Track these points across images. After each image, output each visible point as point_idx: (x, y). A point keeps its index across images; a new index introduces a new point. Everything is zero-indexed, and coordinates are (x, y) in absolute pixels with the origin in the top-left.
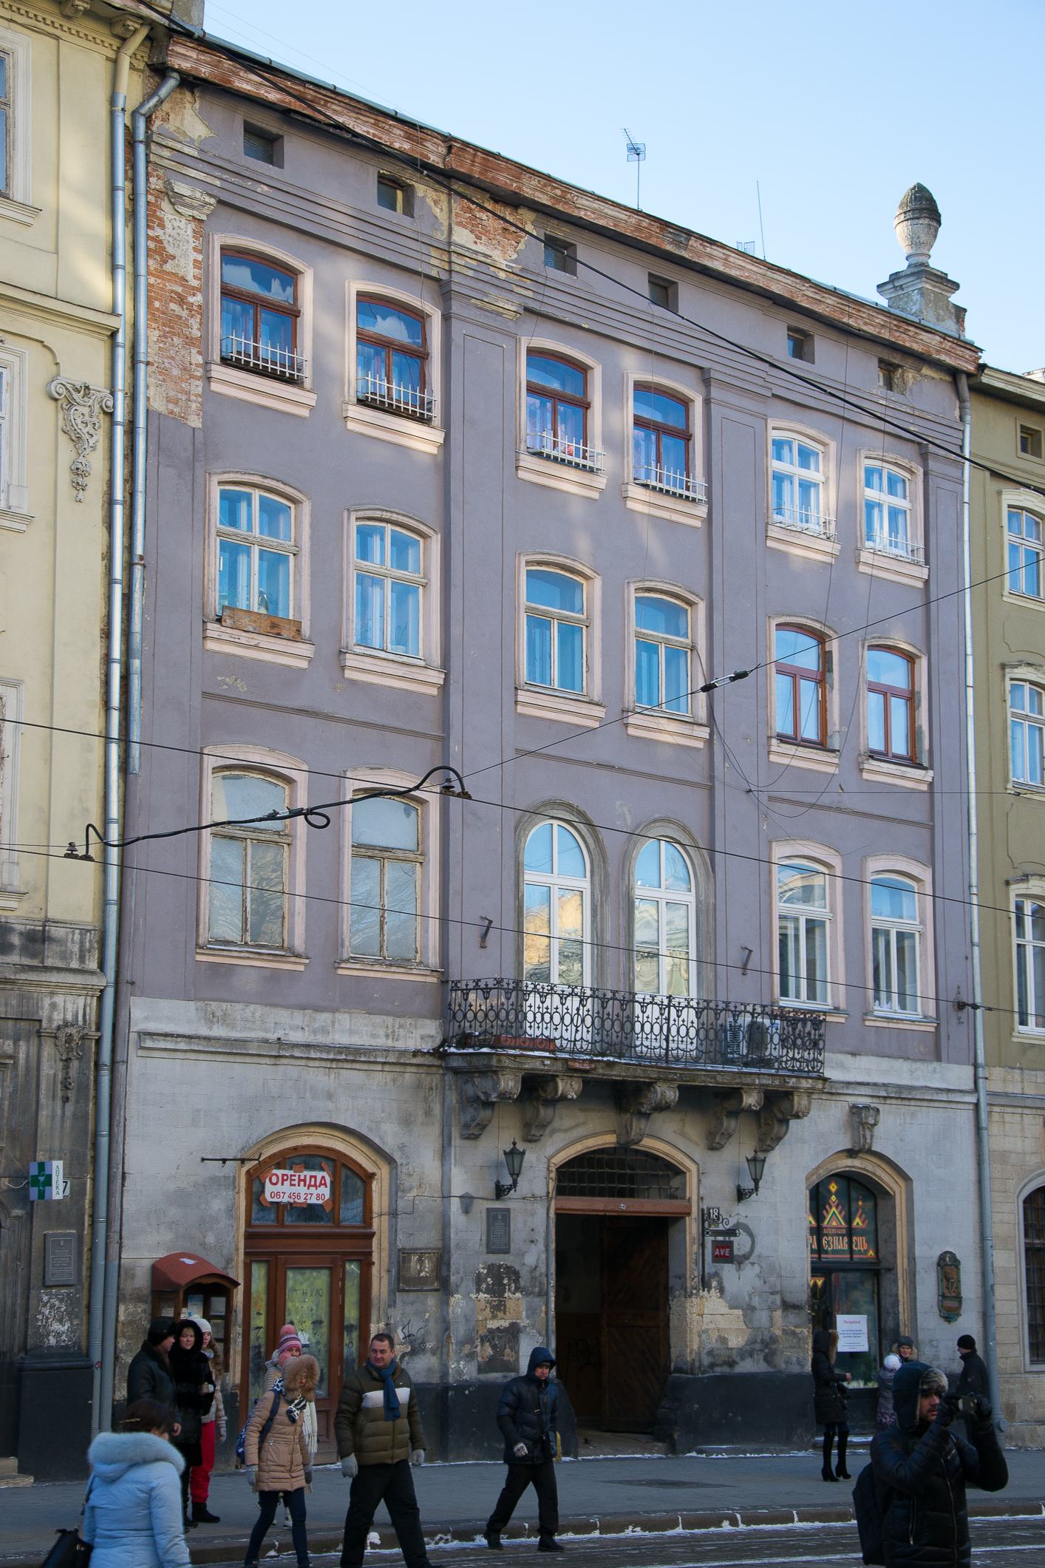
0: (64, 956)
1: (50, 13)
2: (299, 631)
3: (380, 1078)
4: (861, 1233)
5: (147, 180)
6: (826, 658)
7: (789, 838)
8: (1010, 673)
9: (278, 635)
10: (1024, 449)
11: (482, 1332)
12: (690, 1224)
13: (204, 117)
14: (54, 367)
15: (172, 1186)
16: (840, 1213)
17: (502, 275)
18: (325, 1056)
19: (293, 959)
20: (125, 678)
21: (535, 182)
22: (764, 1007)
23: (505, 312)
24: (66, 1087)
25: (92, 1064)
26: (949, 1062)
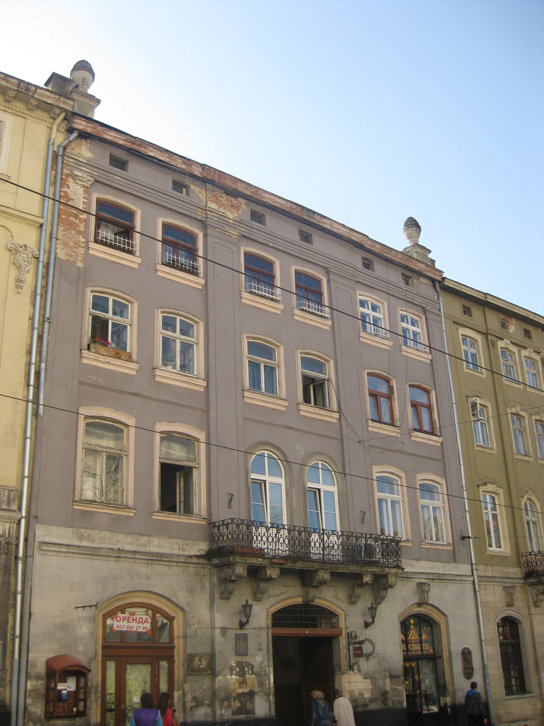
1: (21, 108)
2: (130, 357)
3: (175, 570)
4: (426, 641)
5: (62, 170)
6: (391, 388)
7: (380, 464)
9: (119, 358)
10: (465, 313)
11: (234, 695)
12: (342, 639)
13: (90, 150)
14: (11, 238)
16: (416, 633)
17: (231, 221)
18: (144, 557)
19: (127, 510)
20: (38, 374)
21: (243, 185)
22: (371, 535)
23: (233, 235)
25: (13, 557)
26: (460, 563)
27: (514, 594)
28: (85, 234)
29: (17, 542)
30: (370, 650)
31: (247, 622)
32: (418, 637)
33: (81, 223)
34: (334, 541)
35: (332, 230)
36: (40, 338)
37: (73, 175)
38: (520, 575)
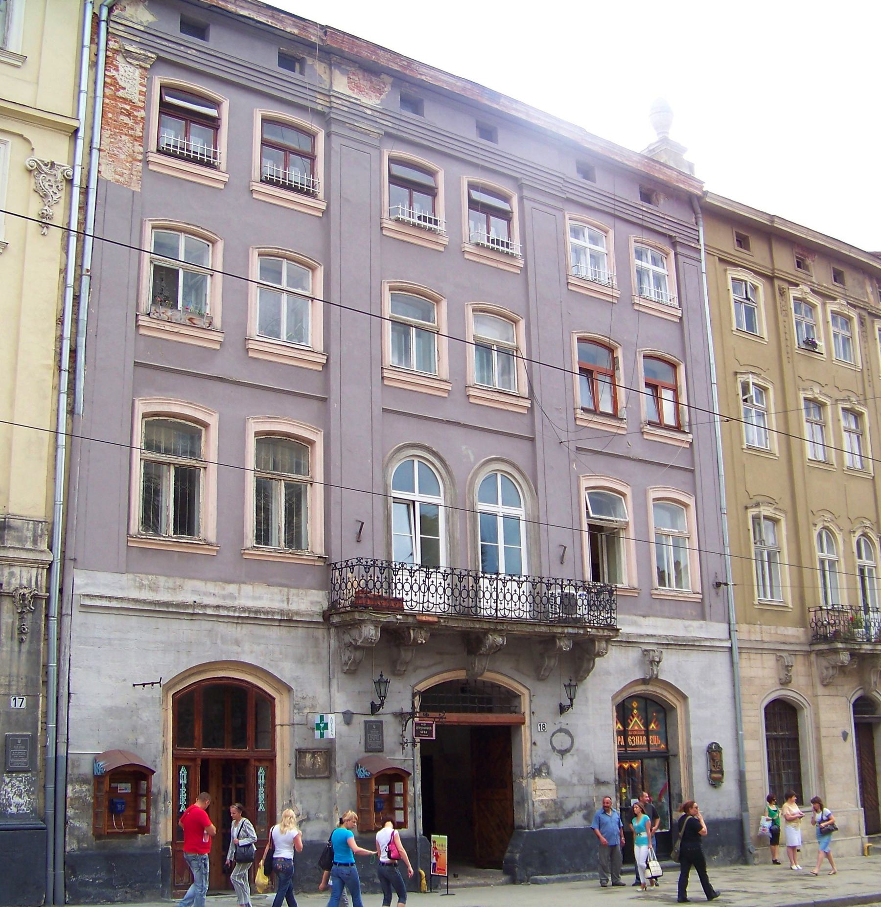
0: (20, 539)
4: (654, 732)
5: (107, 43)
6: (614, 361)
8: (741, 378)
12: (525, 730)
15: (109, 703)
16: (640, 721)
17: (369, 112)
18: (231, 614)
19: (207, 547)
20: (73, 352)
21: (388, 55)
22: (570, 580)
24: (21, 632)
25: (43, 616)
26: (711, 620)
27: (792, 666)
28: (142, 140)
29: (48, 594)
30: (566, 745)
31: (382, 705)
32: (644, 727)
33: (136, 123)
34: (513, 590)
35: (529, 120)
36: (77, 298)
37: (123, 51)
38: (803, 639)
